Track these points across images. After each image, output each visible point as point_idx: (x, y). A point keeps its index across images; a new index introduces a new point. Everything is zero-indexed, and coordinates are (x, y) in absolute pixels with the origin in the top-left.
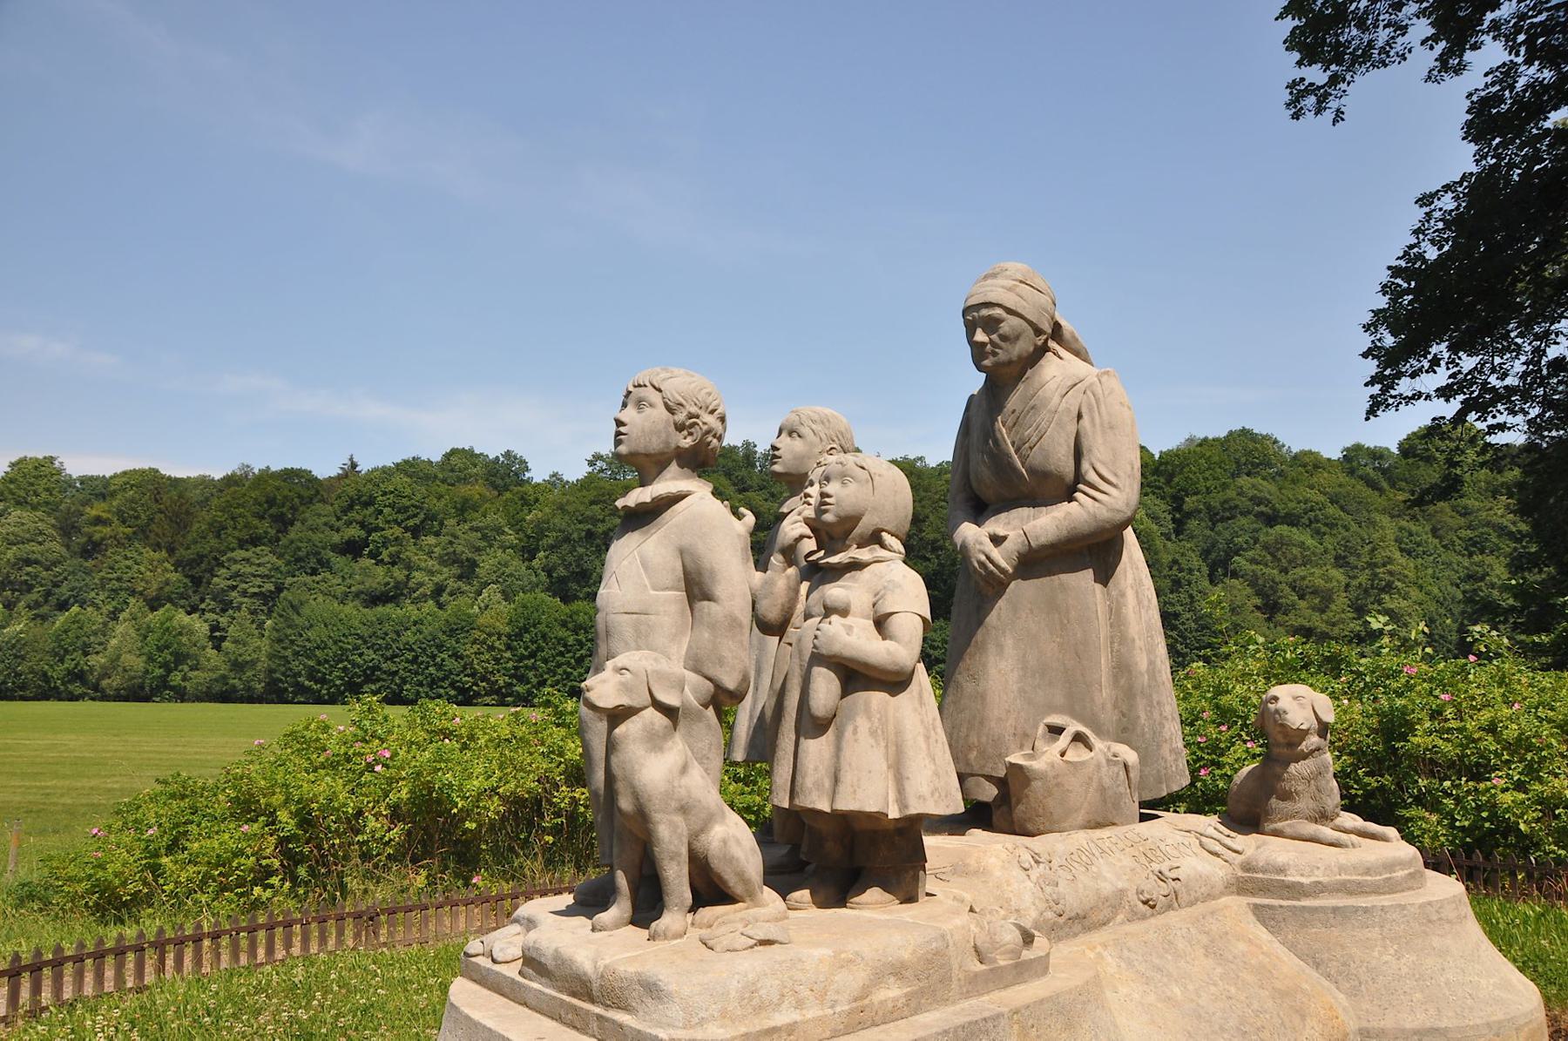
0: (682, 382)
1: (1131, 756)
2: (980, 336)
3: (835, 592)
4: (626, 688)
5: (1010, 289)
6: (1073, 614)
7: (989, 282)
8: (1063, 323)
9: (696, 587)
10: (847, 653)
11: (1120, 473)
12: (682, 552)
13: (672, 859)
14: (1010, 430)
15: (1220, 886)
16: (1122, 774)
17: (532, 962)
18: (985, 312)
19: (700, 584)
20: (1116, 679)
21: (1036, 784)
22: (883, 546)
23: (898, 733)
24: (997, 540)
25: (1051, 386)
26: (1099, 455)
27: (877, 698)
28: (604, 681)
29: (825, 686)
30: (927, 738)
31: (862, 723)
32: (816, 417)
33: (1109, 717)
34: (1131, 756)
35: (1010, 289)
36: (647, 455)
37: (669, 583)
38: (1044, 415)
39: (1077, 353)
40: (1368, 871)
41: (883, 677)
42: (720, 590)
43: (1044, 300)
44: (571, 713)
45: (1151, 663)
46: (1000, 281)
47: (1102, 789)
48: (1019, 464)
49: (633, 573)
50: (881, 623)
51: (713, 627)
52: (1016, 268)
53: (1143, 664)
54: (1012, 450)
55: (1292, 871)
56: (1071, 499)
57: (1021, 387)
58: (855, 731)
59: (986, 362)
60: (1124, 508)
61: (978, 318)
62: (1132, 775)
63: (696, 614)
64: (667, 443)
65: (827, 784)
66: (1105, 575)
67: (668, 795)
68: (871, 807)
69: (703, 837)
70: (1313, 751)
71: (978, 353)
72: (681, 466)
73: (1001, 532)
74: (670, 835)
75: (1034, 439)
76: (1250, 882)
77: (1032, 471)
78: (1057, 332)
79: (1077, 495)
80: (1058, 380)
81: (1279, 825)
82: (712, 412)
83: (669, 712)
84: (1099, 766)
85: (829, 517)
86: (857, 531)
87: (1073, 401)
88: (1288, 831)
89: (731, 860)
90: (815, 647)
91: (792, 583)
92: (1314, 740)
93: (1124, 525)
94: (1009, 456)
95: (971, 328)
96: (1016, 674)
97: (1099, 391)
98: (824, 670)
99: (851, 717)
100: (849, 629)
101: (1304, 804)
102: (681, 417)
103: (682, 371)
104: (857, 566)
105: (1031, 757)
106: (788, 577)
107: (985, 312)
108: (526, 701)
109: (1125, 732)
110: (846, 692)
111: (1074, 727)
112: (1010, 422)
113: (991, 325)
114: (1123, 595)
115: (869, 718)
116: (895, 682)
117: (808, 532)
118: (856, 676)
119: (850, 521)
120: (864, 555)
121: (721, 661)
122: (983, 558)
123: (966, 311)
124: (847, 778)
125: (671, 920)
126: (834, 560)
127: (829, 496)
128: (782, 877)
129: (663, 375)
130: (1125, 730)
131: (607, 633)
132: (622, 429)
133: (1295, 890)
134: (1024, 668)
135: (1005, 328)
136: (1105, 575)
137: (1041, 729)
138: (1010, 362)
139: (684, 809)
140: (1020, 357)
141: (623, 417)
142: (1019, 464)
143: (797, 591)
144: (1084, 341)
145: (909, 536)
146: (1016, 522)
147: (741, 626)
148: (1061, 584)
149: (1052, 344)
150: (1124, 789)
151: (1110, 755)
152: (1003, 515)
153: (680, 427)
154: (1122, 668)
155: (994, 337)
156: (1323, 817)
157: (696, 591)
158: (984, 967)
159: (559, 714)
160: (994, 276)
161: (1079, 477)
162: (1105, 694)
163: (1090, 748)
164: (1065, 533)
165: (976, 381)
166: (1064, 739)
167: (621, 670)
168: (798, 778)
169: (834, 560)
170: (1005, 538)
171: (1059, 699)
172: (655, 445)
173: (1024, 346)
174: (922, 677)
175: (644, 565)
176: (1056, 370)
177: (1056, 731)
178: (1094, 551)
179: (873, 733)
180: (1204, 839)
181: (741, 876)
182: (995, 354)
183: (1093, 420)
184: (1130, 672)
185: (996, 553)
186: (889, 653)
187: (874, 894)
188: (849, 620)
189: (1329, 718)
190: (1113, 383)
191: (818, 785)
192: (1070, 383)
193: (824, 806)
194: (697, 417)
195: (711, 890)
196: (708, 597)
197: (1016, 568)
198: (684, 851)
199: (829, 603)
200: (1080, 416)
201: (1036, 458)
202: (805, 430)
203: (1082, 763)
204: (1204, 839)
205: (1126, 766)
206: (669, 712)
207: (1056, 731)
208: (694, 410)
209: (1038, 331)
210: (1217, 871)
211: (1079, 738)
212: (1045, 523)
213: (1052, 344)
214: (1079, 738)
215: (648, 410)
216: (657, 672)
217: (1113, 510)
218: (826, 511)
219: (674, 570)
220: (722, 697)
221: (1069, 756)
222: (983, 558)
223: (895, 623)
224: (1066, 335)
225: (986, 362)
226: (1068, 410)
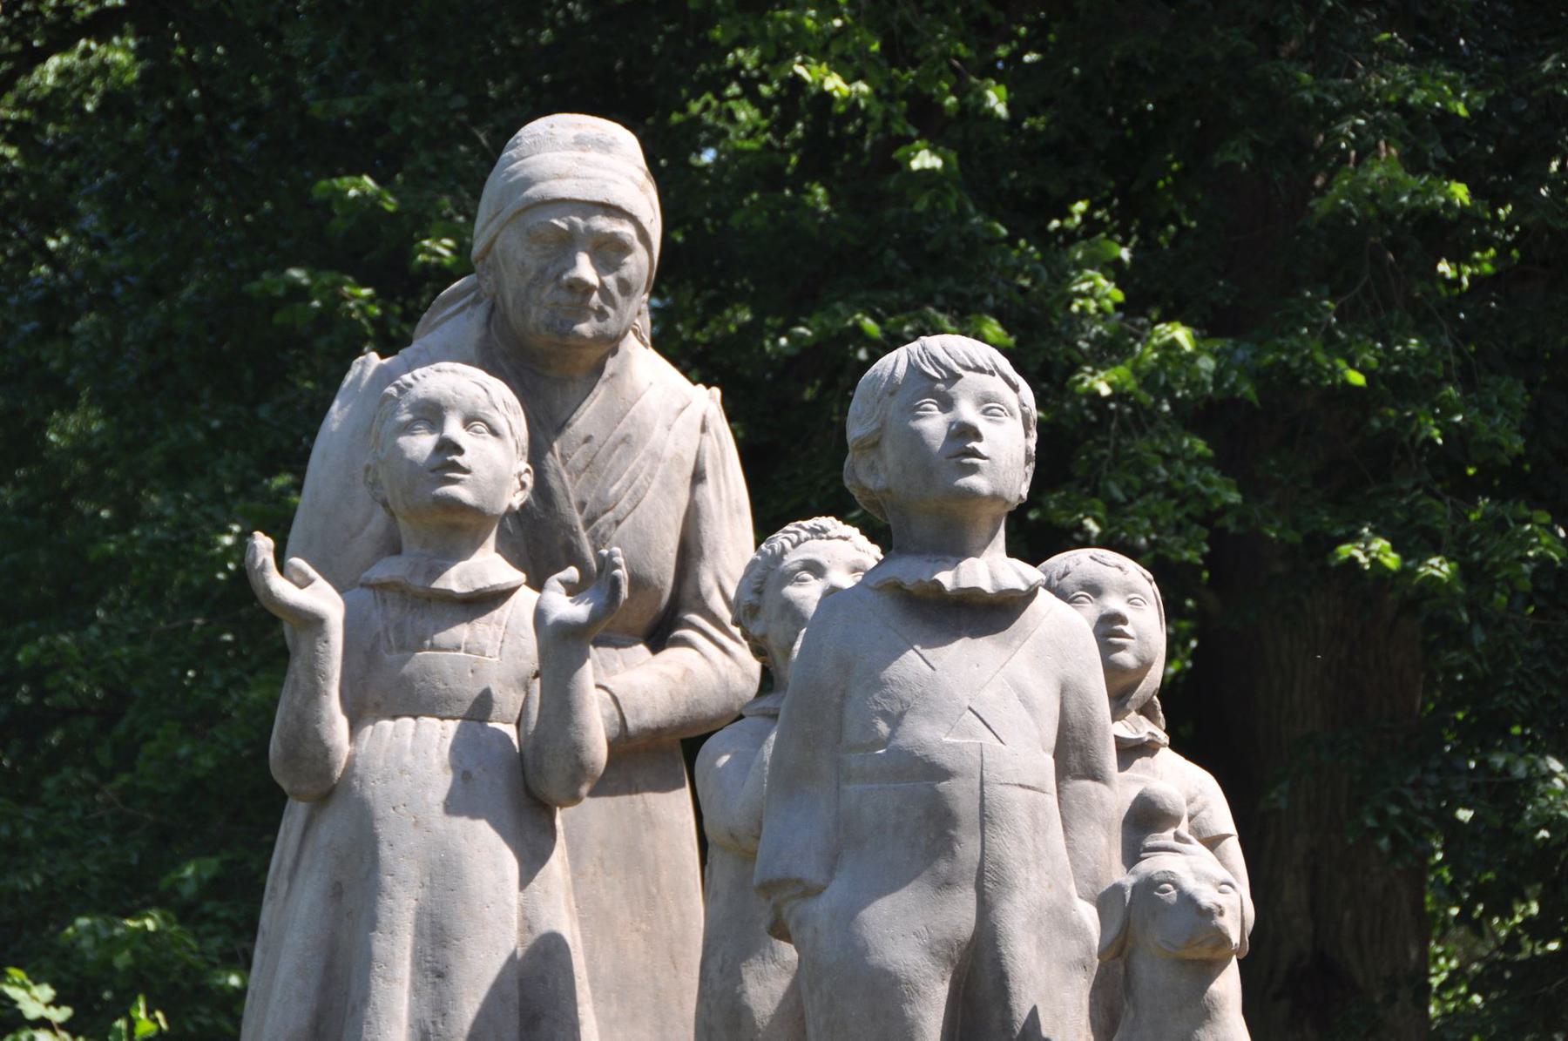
12: (1064, 690)
18: (602, 223)
57: (601, 391)
75: (624, 504)
94: (570, 529)
107: (602, 223)
131: (985, 818)
148: (647, 813)
155: (610, 280)
157: (1074, 760)
182: (601, 315)
183: (718, 491)
200: (698, 477)
218: (1121, 647)
226: (678, 459)
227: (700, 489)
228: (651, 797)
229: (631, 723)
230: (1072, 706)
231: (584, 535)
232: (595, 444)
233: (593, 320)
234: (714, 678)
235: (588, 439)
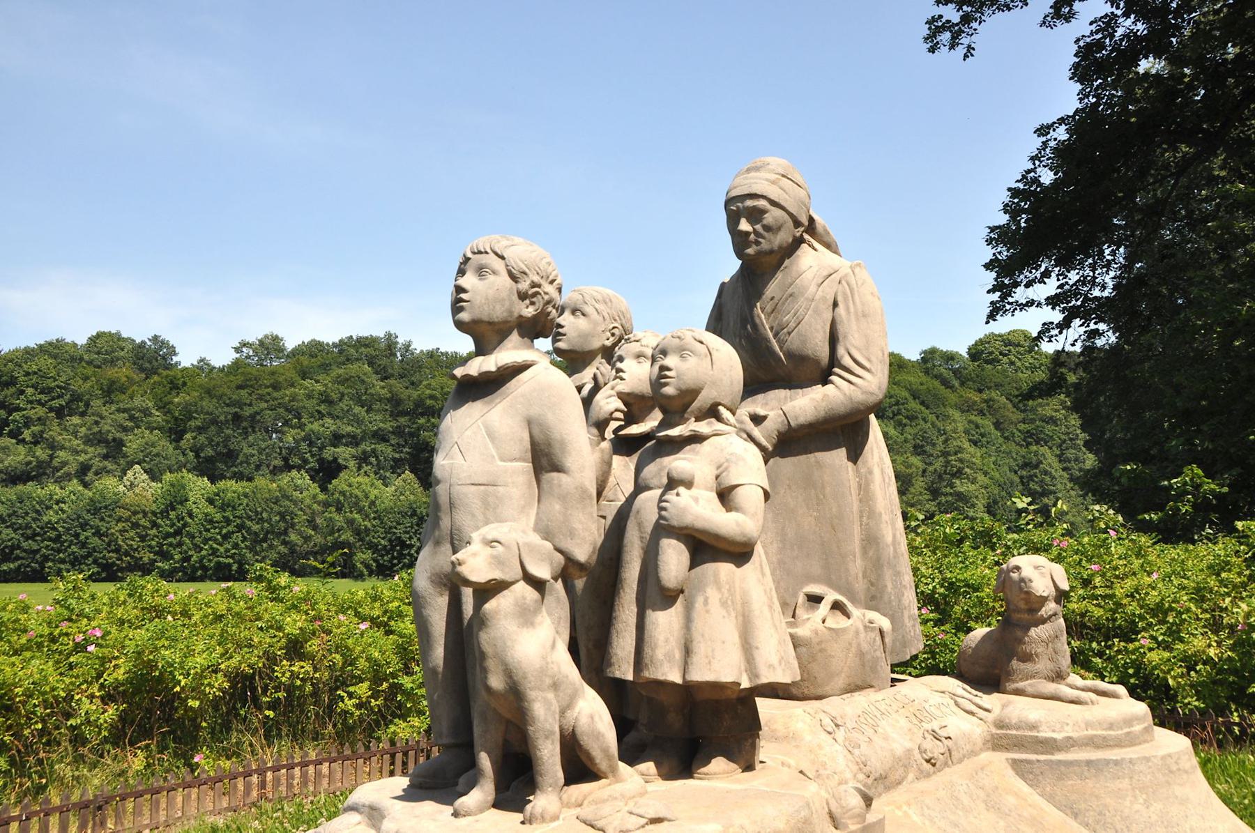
0: (521, 251)
1: (885, 623)
2: (744, 226)
3: (679, 463)
4: (498, 561)
5: (774, 182)
6: (828, 490)
7: (753, 174)
8: (815, 217)
9: (544, 459)
10: (699, 524)
11: (873, 359)
12: (530, 423)
13: (547, 738)
14: (768, 315)
15: (980, 742)
16: (878, 639)
18: (749, 203)
19: (549, 455)
20: (865, 550)
22: (719, 418)
23: (745, 603)
25: (808, 276)
26: (853, 343)
27: (725, 569)
28: (474, 555)
29: (674, 557)
30: (770, 607)
31: (712, 593)
32: (599, 297)
33: (860, 586)
34: (885, 623)
35: (774, 182)
36: (490, 323)
37: (516, 454)
38: (801, 303)
39: (829, 246)
40: (1111, 726)
41: (732, 549)
42: (570, 462)
43: (802, 193)
44: (285, 588)
45: (894, 536)
46: (762, 174)
47: (861, 654)
48: (777, 348)
49: (474, 445)
50: (725, 495)
51: (563, 498)
52: (777, 162)
54: (771, 335)
55: (1043, 727)
56: (825, 381)
57: (779, 275)
58: (706, 602)
59: (750, 251)
60: (877, 391)
61: (739, 209)
62: (887, 640)
63: (545, 485)
64: (511, 312)
65: (678, 655)
66: (854, 456)
67: (543, 671)
68: (727, 677)
69: (571, 715)
70: (1051, 616)
71: (740, 242)
73: (762, 412)
74: (544, 714)
75: (792, 324)
77: (789, 355)
78: (811, 227)
79: (833, 378)
80: (814, 269)
81: (1021, 685)
82: (552, 282)
84: (857, 632)
85: (669, 390)
86: (696, 405)
87: (828, 290)
88: (1029, 690)
89: (598, 736)
90: (661, 517)
91: (606, 457)
92: (1051, 606)
94: (767, 340)
95: (732, 220)
96: (775, 545)
97: (853, 282)
98: (674, 542)
99: (701, 587)
100: (696, 500)
101: (1043, 665)
102: (524, 285)
103: (521, 240)
104: (697, 439)
106: (602, 451)
107: (749, 203)
108: (241, 576)
109: (873, 601)
110: (693, 566)
111: (831, 596)
112: (769, 308)
113: (755, 215)
114: (871, 472)
115: (719, 589)
116: (739, 553)
118: (705, 547)
119: (690, 394)
120: (703, 427)
121: (572, 534)
123: (729, 202)
124: (700, 649)
125: (541, 802)
126: (675, 432)
127: (669, 369)
129: (504, 243)
130: (873, 598)
131: (452, 505)
132: (463, 296)
133: (1049, 745)
134: (783, 541)
135: (768, 219)
136: (854, 456)
137: (801, 599)
138: (771, 252)
139: (555, 686)
140: (780, 247)
141: (463, 282)
142: (777, 348)
143: (609, 464)
144: (836, 235)
146: (774, 403)
148: (817, 462)
149: (806, 236)
150: (880, 653)
152: (760, 396)
153: (522, 296)
154: (871, 540)
155: (758, 227)
156: (1059, 677)
157: (544, 462)
159: (272, 589)
160: (757, 169)
161: (834, 361)
162: (857, 566)
163: (847, 615)
164: (822, 413)
165: (731, 266)
166: (824, 607)
167: (491, 543)
168: (647, 650)
169: (675, 432)
171: (816, 569)
172: (499, 313)
173: (783, 237)
175: (491, 435)
176: (810, 260)
177: (815, 600)
178: (844, 431)
179: (724, 604)
180: (959, 700)
181: (605, 751)
182: (757, 243)
183: (848, 309)
184: (878, 544)
186: (738, 524)
187: (719, 764)
188: (694, 491)
189: (1065, 586)
190: (863, 274)
191: (669, 656)
192: (826, 273)
193: (679, 680)
194: (539, 286)
195: (579, 768)
196: (558, 468)
197: (775, 446)
198: (557, 729)
199: (675, 475)
200: (835, 305)
201: (793, 342)
202: (588, 309)
203: (844, 630)
204: (959, 700)
205: (881, 632)
207: (815, 600)
208: (536, 279)
209: (797, 223)
211: (836, 606)
213: (806, 236)
214: (836, 606)
215: (491, 278)
216: (528, 545)
217: (864, 392)
218: (666, 384)
219: (521, 440)
220: (571, 570)
221: (829, 623)
223: (741, 495)
224: (819, 228)
225: (750, 251)
226: (824, 299)
227: (837, 310)
228: (820, 455)
229: (792, 424)
230: (536, 432)
231: (774, 341)
232: (776, 300)
233: (754, 246)
234: (842, 397)
235: (772, 299)
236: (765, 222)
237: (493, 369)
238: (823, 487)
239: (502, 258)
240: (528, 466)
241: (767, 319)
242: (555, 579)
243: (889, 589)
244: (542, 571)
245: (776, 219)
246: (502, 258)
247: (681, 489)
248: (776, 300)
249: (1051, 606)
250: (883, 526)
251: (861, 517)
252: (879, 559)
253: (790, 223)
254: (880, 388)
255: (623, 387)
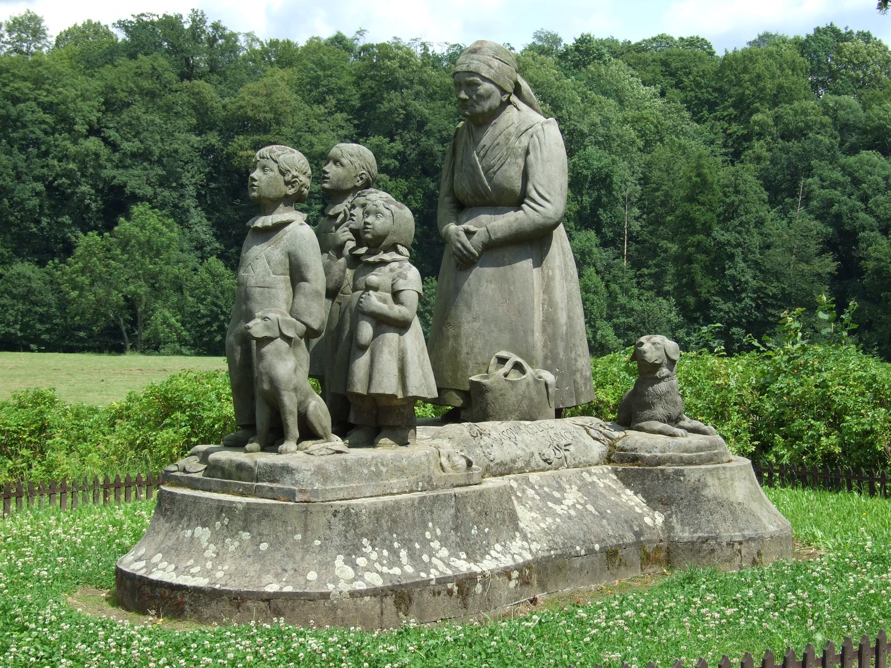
3: (373, 278)
4: (268, 328)
9: (296, 274)
15: (596, 458)
17: (214, 469)
21: (489, 396)
24: (469, 234)
33: (539, 352)
36: (269, 199)
37: (281, 271)
42: (310, 275)
48: (486, 183)
50: (396, 295)
53: (563, 318)
54: (482, 173)
57: (490, 129)
62: (550, 390)
72: (286, 206)
73: (472, 228)
74: (290, 402)
76: (616, 457)
79: (524, 206)
83: (288, 339)
88: (646, 427)
89: (318, 416)
91: (342, 268)
92: (665, 371)
93: (556, 225)
97: (542, 137)
101: (660, 410)
102: (288, 177)
104: (384, 263)
105: (486, 377)
112: (482, 153)
116: (402, 326)
117: (351, 236)
120: (386, 257)
121: (311, 315)
122: (460, 246)
126: (371, 259)
128: (342, 428)
137: (493, 361)
138: (483, 113)
139: (295, 390)
142: (486, 183)
145: (413, 245)
147: (321, 295)
151: (536, 377)
153: (287, 183)
154: (549, 320)
158: (444, 474)
162: (538, 338)
163: (523, 372)
166: (508, 366)
169: (371, 259)
170: (474, 233)
172: (273, 193)
174: (416, 325)
177: (502, 361)
178: (534, 242)
184: (554, 324)
185: (468, 244)
194: (297, 177)
195: (308, 433)
196: (304, 279)
201: (499, 178)
202: (345, 161)
205: (546, 385)
206: (288, 339)
207: (502, 361)
208: (295, 173)
209: (503, 91)
210: (597, 449)
211: (517, 366)
212: (502, 223)
213: (514, 98)
214: (517, 366)
222: (460, 246)
223: (403, 296)
229: (493, 237)
232: (486, 148)
235: (484, 146)
236: (478, 92)
237: (270, 224)
238: (514, 283)
239: (276, 162)
240: (288, 277)
241: (481, 162)
242: (301, 338)
243: (561, 356)
244: (290, 333)
245: (487, 91)
246: (276, 162)
247: (371, 292)
248: (486, 148)
249: (665, 371)
250: (559, 311)
251: (543, 304)
252: (554, 334)
253: (497, 92)
254: (556, 214)
255: (352, 226)
